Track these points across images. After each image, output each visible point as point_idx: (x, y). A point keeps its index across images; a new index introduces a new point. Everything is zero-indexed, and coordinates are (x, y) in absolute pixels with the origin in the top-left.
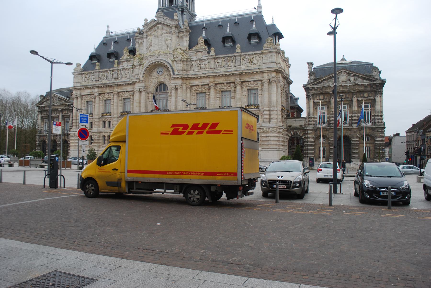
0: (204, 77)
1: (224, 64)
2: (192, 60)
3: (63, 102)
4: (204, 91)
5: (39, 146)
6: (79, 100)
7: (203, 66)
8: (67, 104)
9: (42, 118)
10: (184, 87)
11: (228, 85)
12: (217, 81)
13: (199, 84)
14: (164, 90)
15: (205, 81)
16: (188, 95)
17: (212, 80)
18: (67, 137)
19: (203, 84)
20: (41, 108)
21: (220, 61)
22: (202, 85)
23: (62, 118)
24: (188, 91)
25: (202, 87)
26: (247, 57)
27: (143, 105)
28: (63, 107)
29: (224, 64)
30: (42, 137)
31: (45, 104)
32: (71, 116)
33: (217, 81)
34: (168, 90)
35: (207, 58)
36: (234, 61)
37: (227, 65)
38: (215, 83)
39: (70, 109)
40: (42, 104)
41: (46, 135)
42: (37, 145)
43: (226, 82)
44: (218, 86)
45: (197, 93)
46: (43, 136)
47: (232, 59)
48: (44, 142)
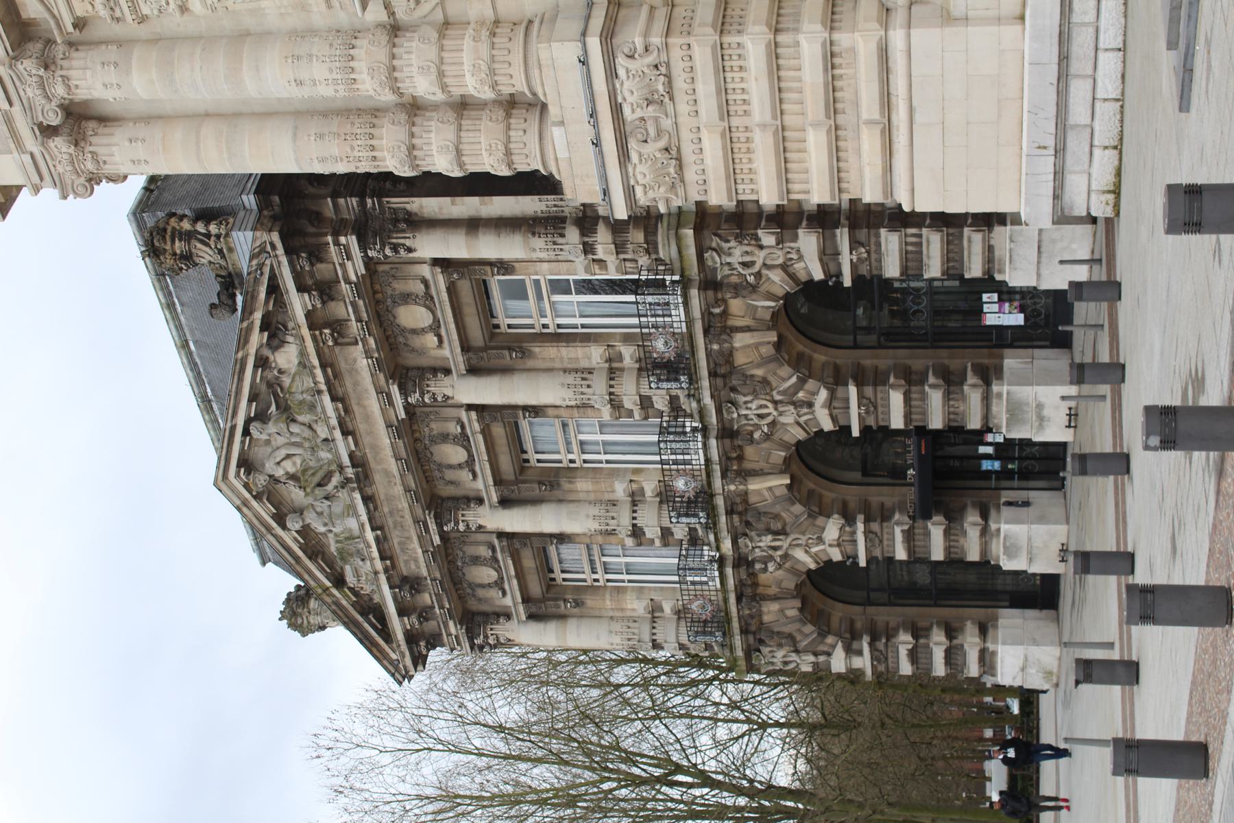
3: (287, 358)
5: (880, 635)
6: (91, 80)
8: (298, 304)
9: (548, 601)
18: (744, 289)
20: (425, 614)
23: (505, 371)
28: (360, 363)
30: (770, 611)
31: (367, 574)
32: (457, 247)
39: (356, 268)
40: (374, 612)
41: (741, 561)
42: (863, 662)
46: (749, 592)
48: (828, 585)
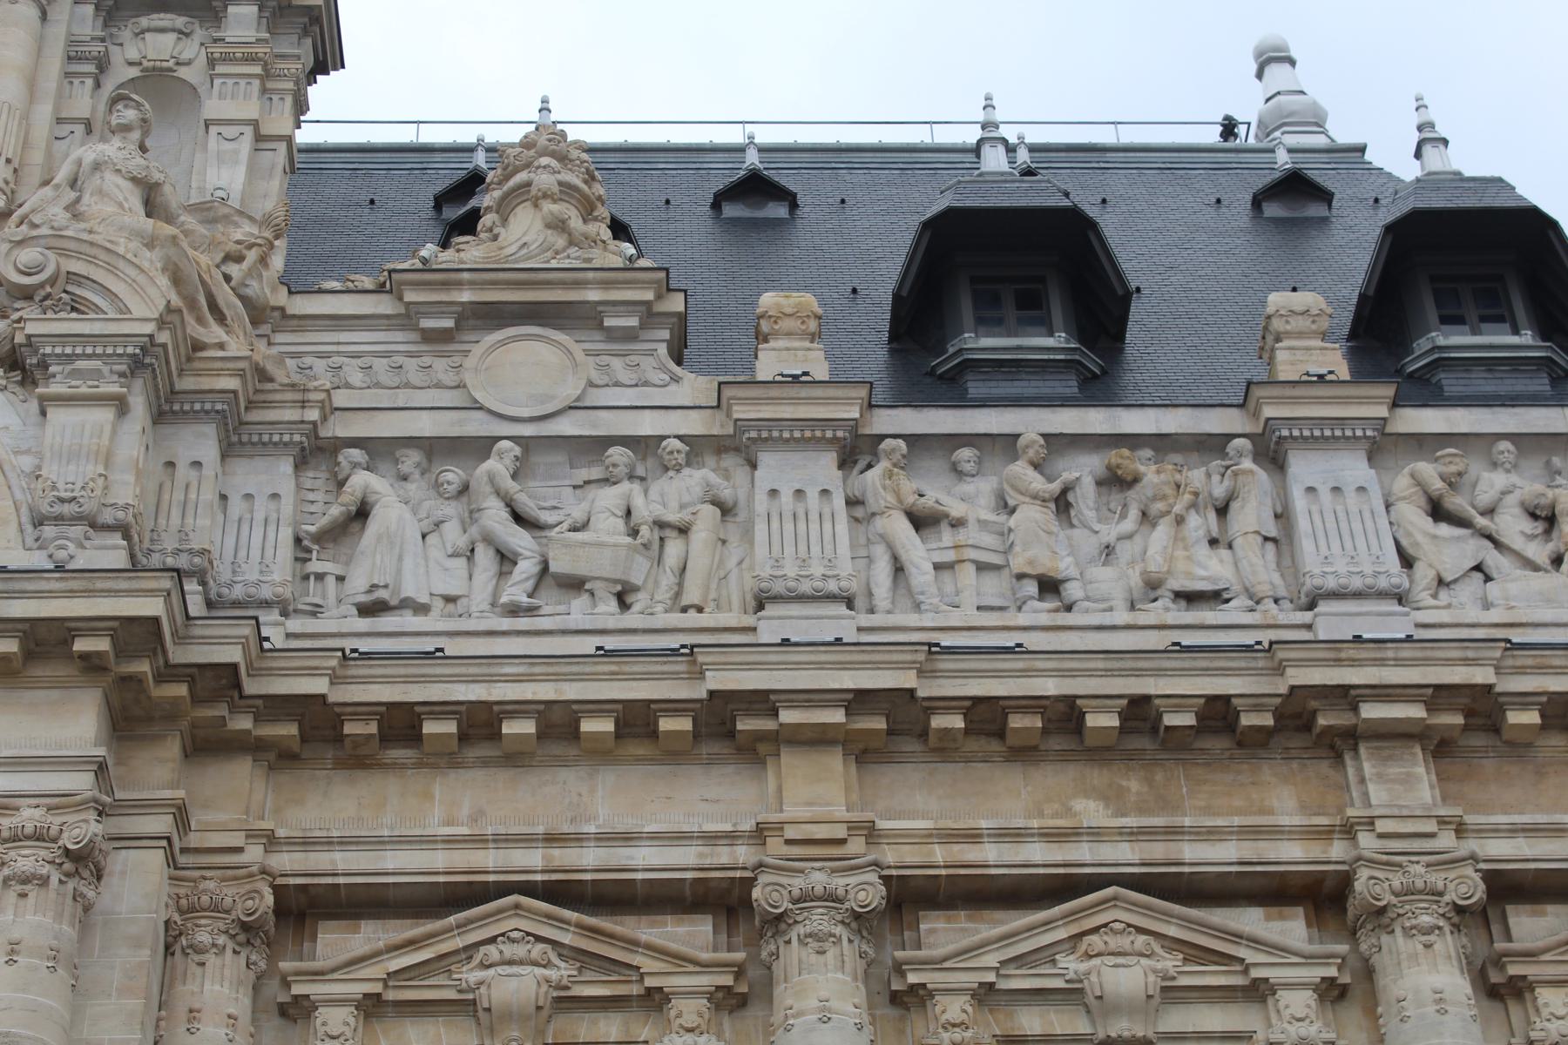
0: (636, 721)
1: (1039, 542)
2: (340, 428)
7: (600, 546)
10: (138, 885)
11: (1175, 921)
12: (936, 816)
13: (489, 862)
15: (665, 820)
17: (813, 792)
19: (588, 860)
21: (968, 497)
24: (220, 986)
25: (568, 926)
26: (1490, 483)
29: (1039, 542)
33: (936, 816)
35: (694, 424)
36: (1252, 515)
37: (1112, 582)
38: (890, 855)
43: (1124, 855)
44: (942, 933)
47: (1200, 476)
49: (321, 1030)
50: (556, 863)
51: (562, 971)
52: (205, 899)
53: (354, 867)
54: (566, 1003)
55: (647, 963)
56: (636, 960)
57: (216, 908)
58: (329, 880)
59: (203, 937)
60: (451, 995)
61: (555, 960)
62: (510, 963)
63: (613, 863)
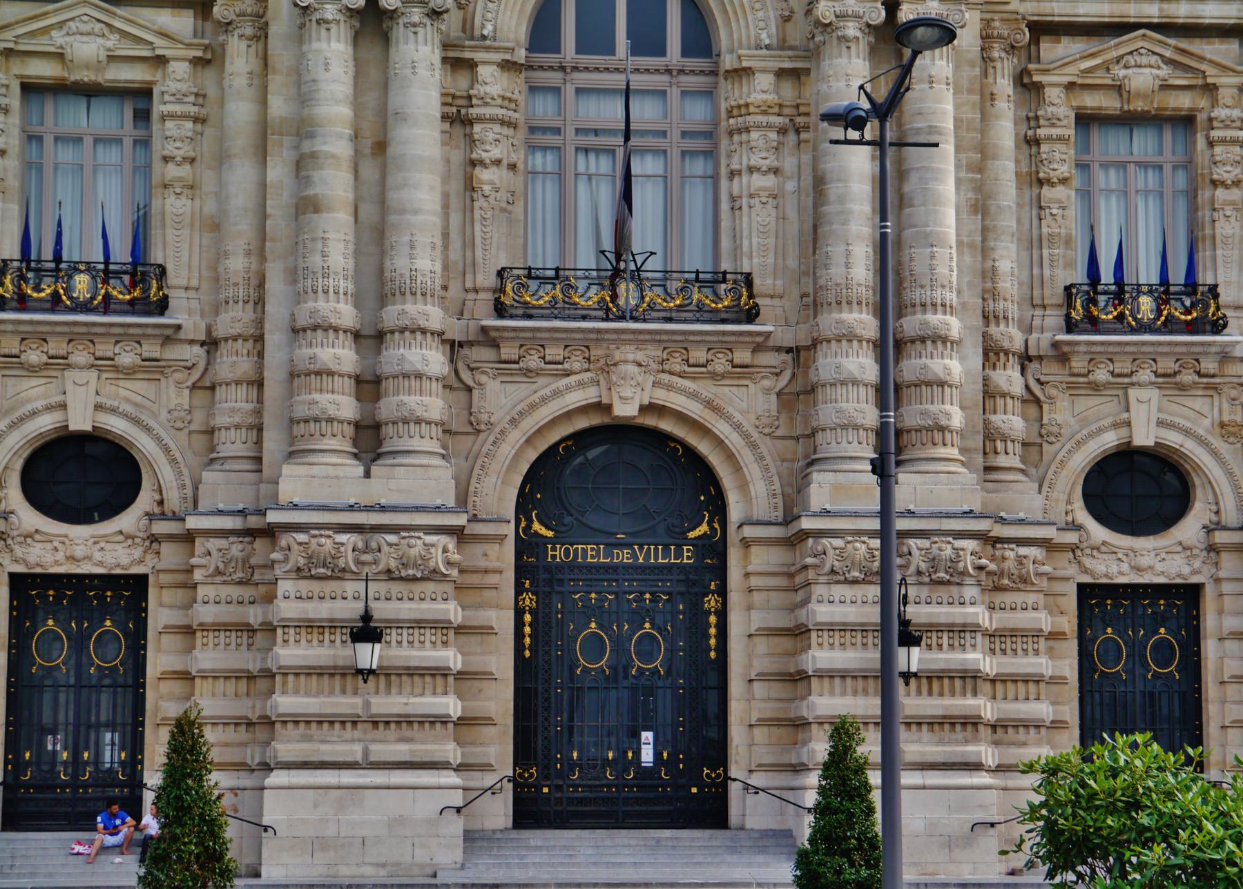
4: (1184, 101)
13: (1132, 12)
14: (647, 40)
16: (1005, 132)
22: (1166, 28)
25: (1169, 46)
27: (423, 192)
34: (700, 39)
45: (1085, 120)
49: (1047, 100)
50: (1165, 13)
51: (1165, 71)
52: (995, 33)
53: (1063, 12)
54: (1165, 87)
55: (1210, 70)
56: (1203, 67)
57: (1000, 37)
58: (1050, 19)
59: (996, 54)
60: (1109, 82)
61: (1162, 65)
62: (1140, 66)
63: (1195, 14)
